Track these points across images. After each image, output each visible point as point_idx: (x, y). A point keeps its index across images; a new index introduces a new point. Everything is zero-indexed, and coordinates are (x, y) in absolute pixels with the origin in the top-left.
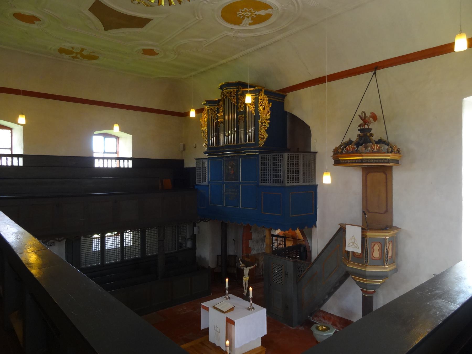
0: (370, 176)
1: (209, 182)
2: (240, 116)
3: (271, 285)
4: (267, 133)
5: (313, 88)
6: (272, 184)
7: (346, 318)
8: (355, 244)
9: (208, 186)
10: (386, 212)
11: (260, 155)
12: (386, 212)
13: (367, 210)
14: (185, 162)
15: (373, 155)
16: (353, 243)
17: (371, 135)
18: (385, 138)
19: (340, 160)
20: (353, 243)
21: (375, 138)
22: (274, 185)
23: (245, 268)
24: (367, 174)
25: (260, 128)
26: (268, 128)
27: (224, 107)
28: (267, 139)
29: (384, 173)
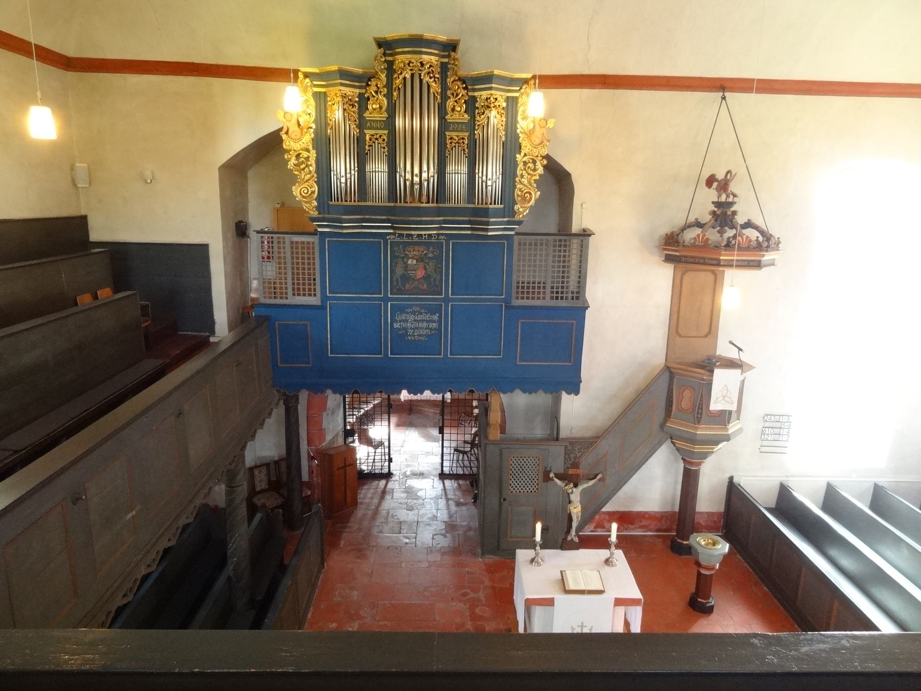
0: (688, 278)
1: (324, 298)
2: (454, 134)
3: (505, 500)
4: (538, 188)
5: (586, 92)
6: (549, 303)
7: (622, 509)
8: (726, 399)
9: (322, 307)
10: (709, 332)
11: (516, 238)
12: (709, 332)
13: (677, 332)
14: (92, 223)
15: (708, 243)
16: (724, 397)
17: (734, 213)
18: (759, 222)
19: (719, 260)
20: (724, 397)
21: (740, 219)
22: (553, 303)
23: (574, 490)
24: (683, 274)
25: (519, 173)
26: (540, 175)
27: (389, 96)
28: (537, 201)
29: (713, 272)
